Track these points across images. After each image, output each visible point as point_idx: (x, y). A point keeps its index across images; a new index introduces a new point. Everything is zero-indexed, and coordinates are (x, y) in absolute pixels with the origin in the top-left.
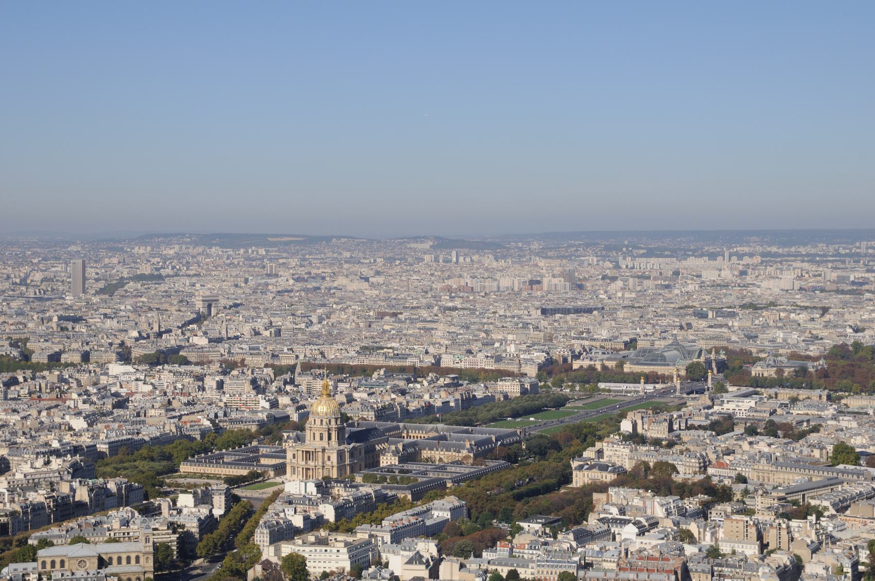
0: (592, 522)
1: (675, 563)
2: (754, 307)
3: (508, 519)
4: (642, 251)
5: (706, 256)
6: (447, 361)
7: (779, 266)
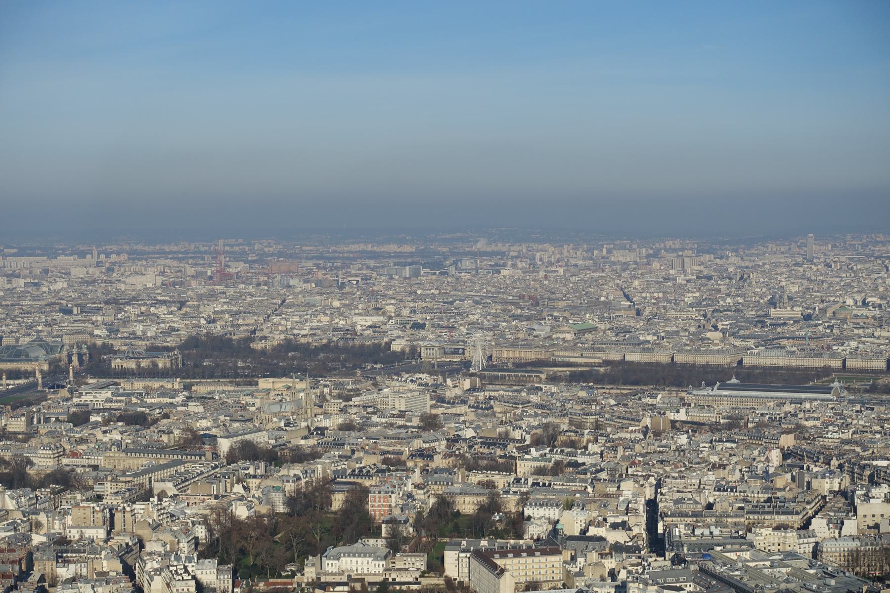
2: (116, 302)
5: (75, 254)
7: (144, 262)
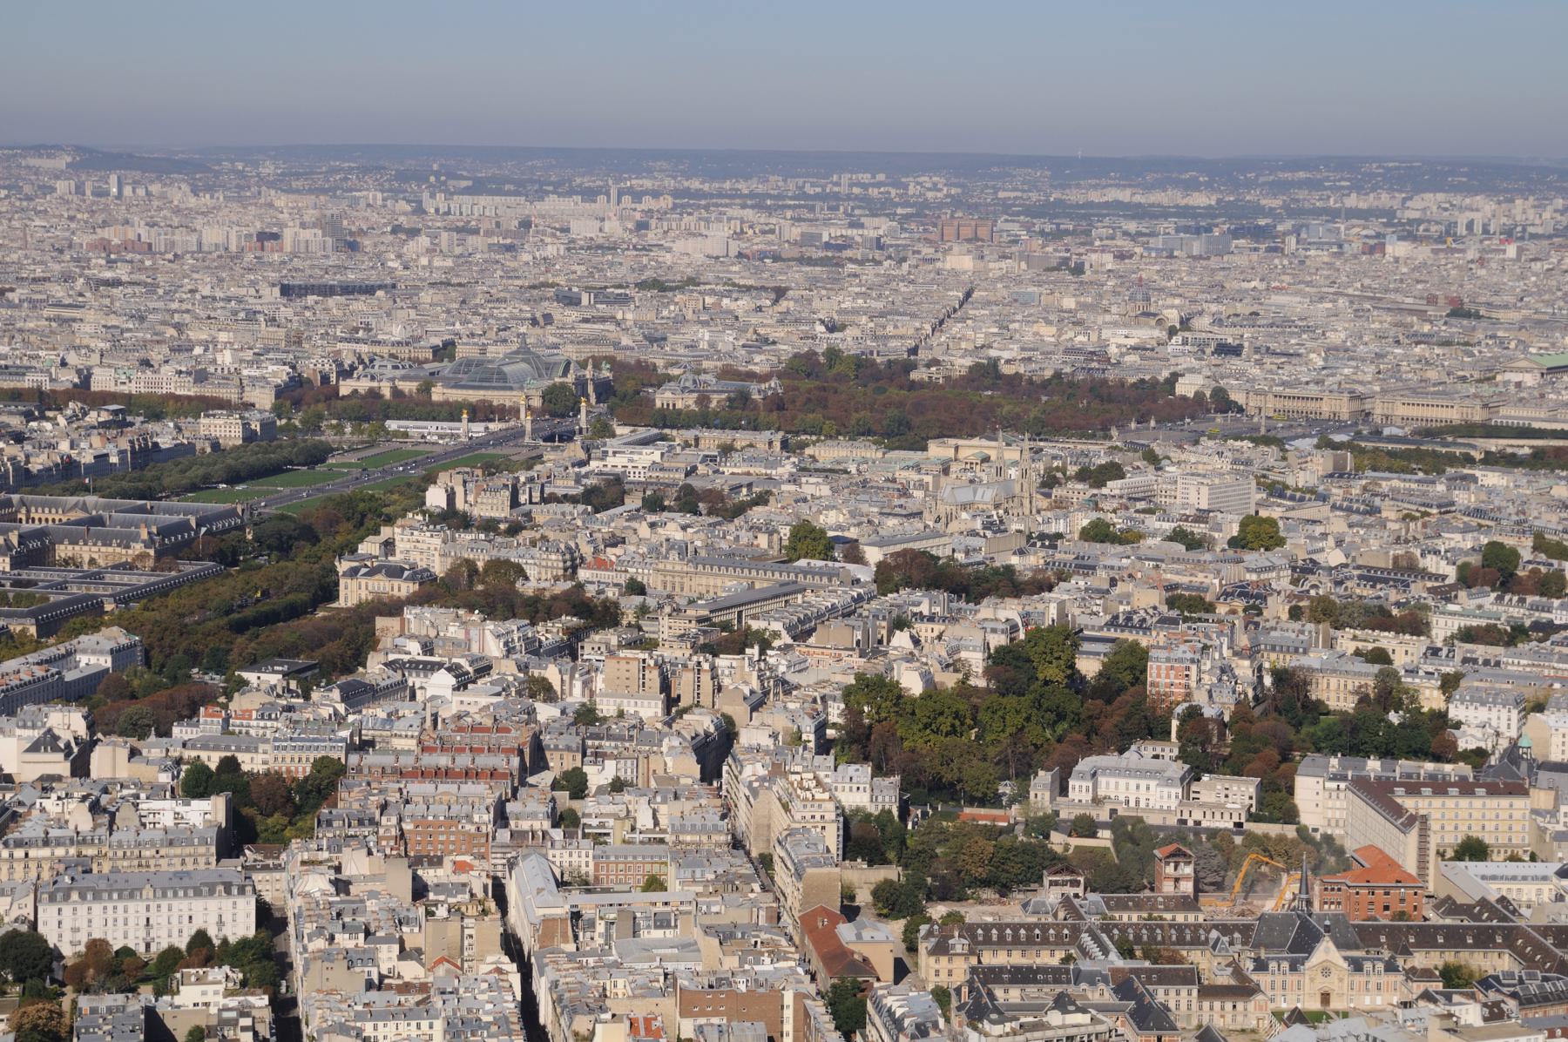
0: (374, 669)
1: (519, 736)
2: (659, 286)
3: (220, 666)
4: (464, 184)
5: (577, 193)
6: (102, 381)
